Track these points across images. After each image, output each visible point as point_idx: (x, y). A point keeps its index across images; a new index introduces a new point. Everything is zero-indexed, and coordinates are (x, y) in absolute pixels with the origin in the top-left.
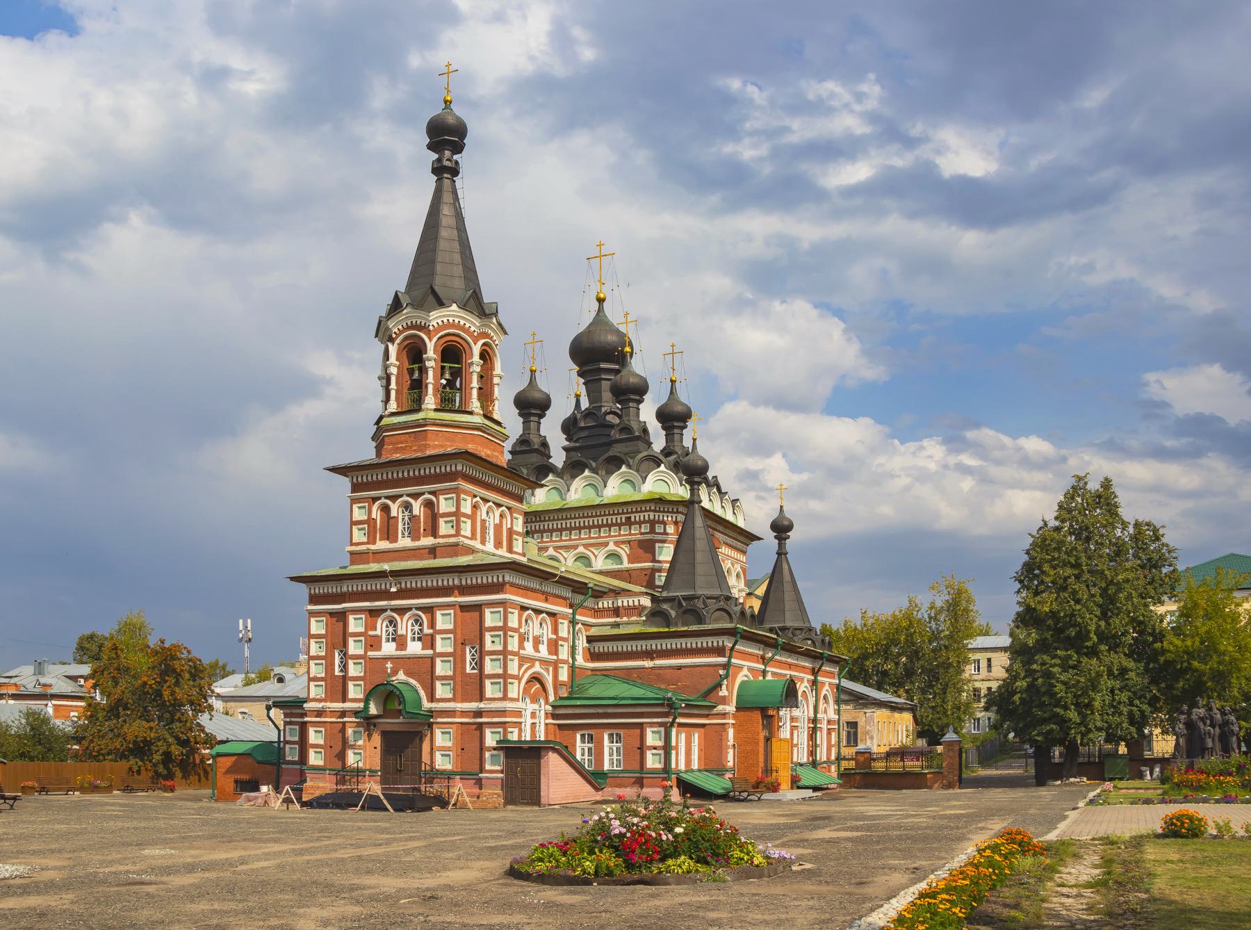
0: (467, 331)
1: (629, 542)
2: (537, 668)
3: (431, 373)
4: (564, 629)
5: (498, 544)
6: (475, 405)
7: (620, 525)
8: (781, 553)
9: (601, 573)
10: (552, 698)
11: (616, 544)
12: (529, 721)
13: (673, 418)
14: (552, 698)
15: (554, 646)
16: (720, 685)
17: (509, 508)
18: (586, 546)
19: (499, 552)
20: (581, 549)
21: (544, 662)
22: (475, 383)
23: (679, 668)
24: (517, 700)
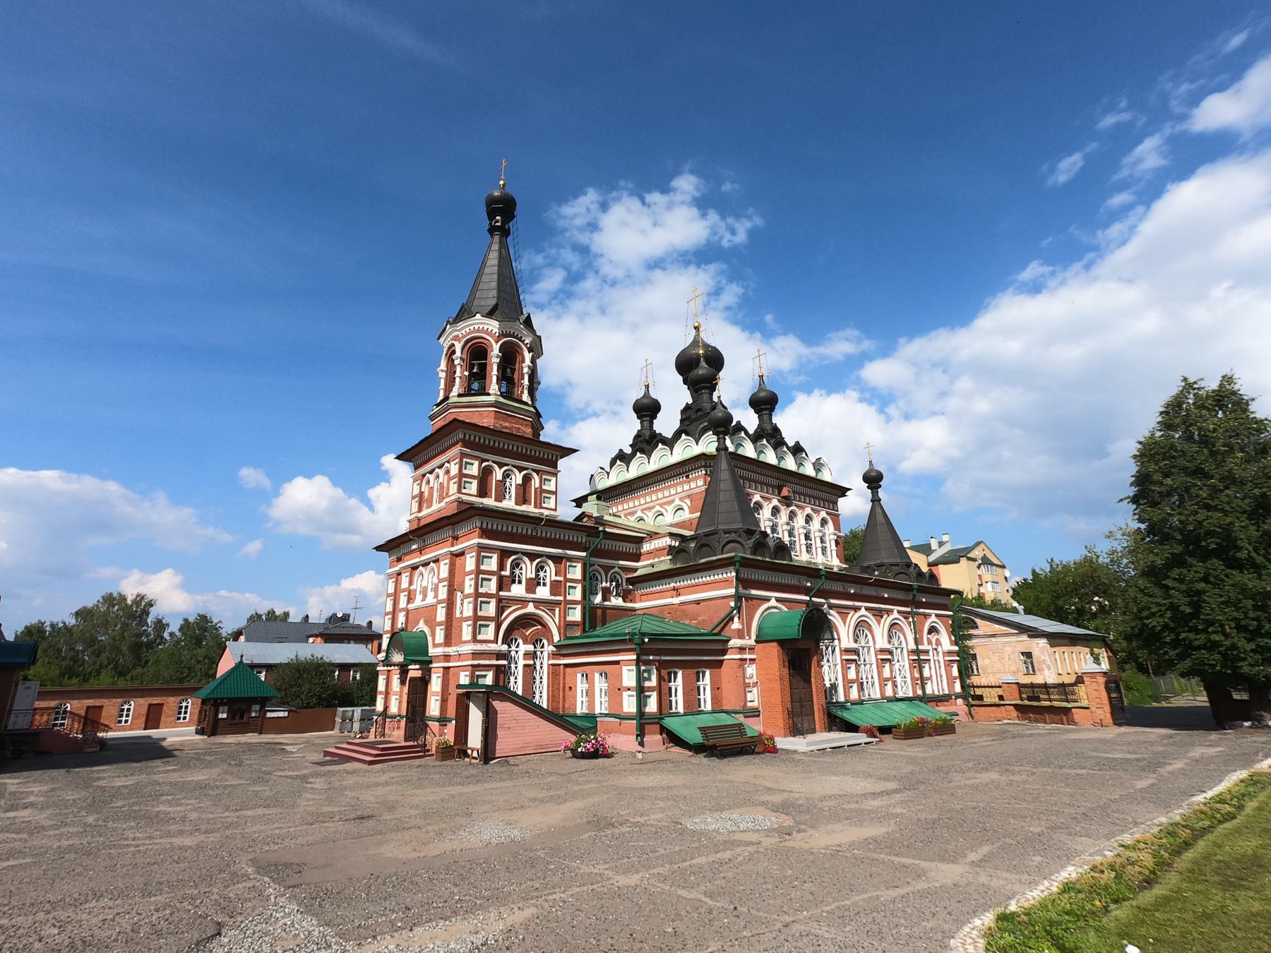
0: (490, 333)
1: (688, 496)
2: (531, 608)
3: (458, 369)
4: (576, 572)
5: (523, 499)
6: (494, 387)
7: (682, 483)
8: (876, 500)
9: (671, 525)
10: (556, 638)
11: (681, 499)
12: (521, 663)
13: (764, 403)
14: (556, 638)
15: (556, 587)
16: (732, 619)
17: (537, 472)
18: (661, 505)
19: (524, 508)
20: (658, 508)
21: (538, 603)
22: (495, 371)
23: (698, 602)
24: (496, 641)
